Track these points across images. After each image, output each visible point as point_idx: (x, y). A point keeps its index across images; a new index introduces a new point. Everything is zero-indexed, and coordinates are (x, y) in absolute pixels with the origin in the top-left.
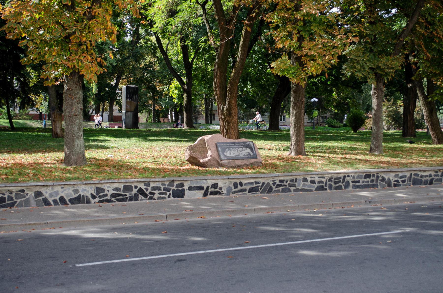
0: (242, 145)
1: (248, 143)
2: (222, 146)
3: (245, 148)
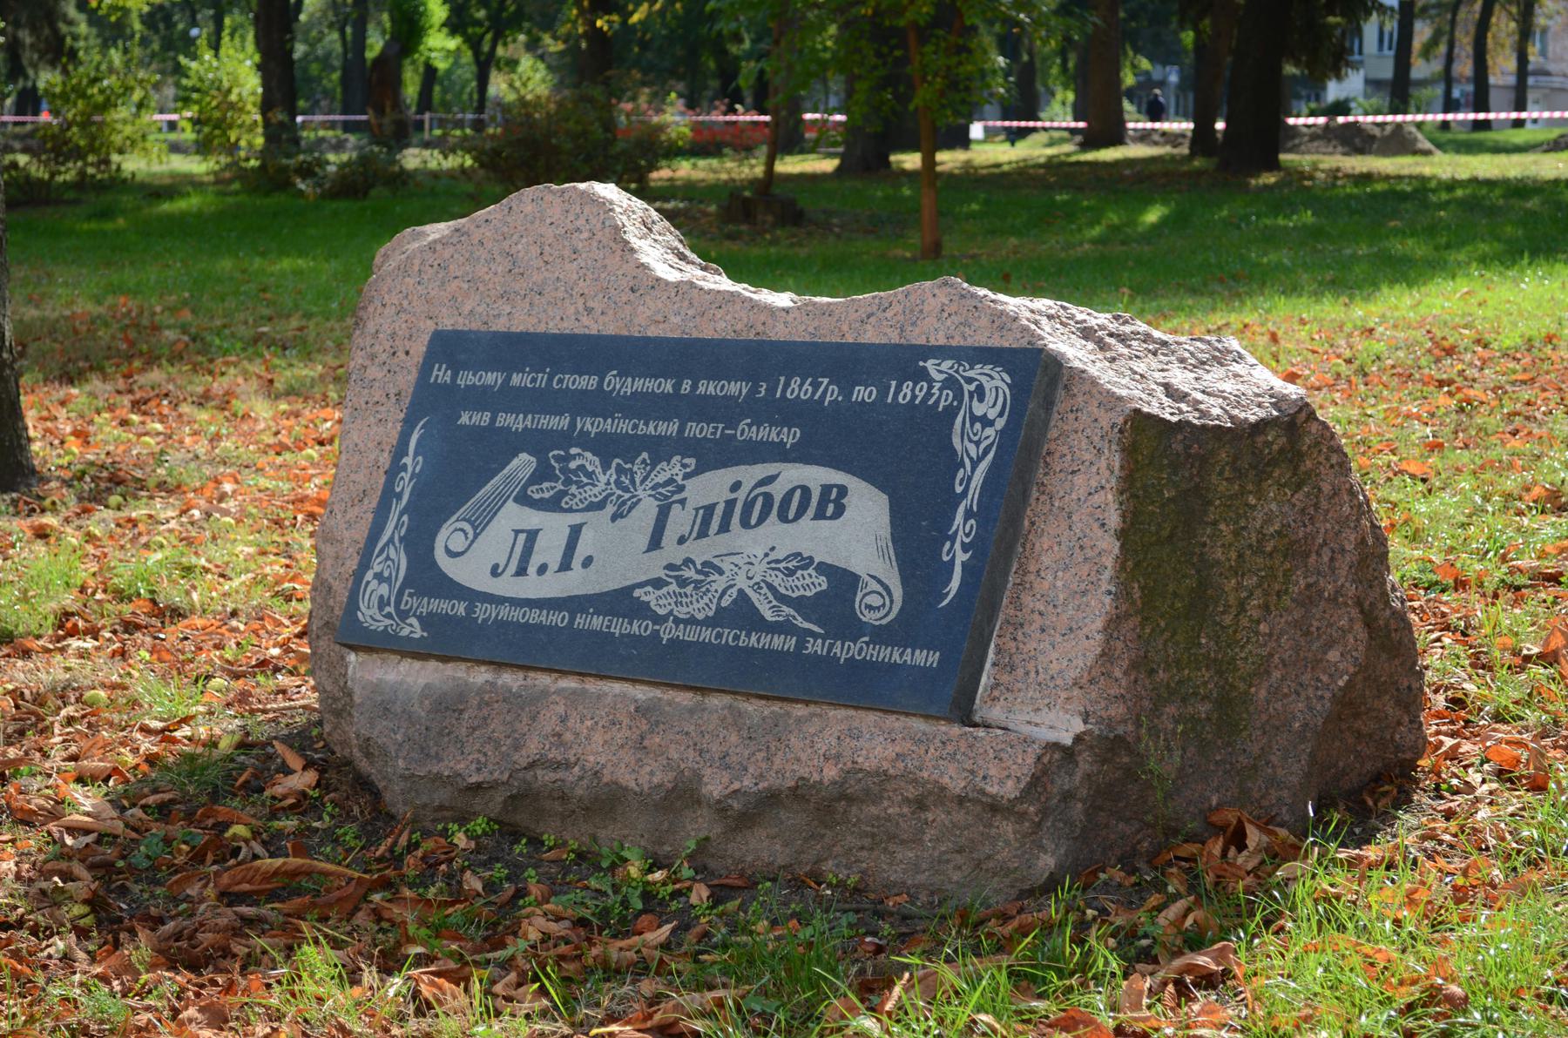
0: (787, 413)
1: (937, 369)
3: (816, 476)
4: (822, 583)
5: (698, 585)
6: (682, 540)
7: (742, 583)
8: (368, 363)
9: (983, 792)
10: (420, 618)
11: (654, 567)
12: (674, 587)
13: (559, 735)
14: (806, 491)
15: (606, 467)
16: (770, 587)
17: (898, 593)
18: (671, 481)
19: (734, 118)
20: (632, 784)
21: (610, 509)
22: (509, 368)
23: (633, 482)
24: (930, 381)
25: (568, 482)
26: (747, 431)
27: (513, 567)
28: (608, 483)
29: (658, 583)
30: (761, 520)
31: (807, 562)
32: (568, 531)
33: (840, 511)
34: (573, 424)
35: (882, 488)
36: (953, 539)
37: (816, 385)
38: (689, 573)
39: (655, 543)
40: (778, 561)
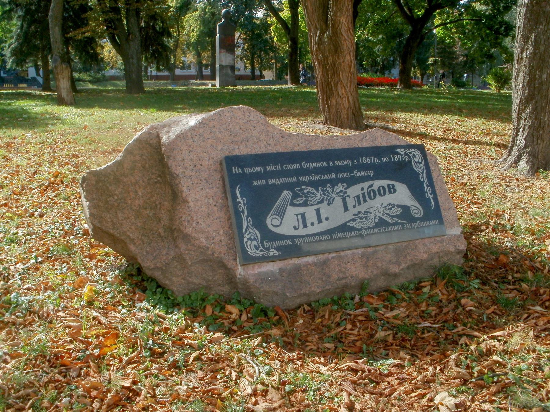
0: (366, 167)
1: (401, 151)
2: (258, 176)
3: (385, 183)
4: (400, 210)
5: (366, 218)
6: (354, 207)
7: (378, 215)
8: (185, 170)
9: (458, 250)
10: (275, 248)
11: (349, 216)
12: (359, 220)
13: (340, 270)
14: (383, 187)
15: (318, 191)
16: (387, 214)
17: (421, 208)
18: (341, 191)
19: (284, 86)
20: (367, 277)
21: (326, 203)
22: (264, 165)
23: (328, 193)
24: (401, 154)
25: (306, 197)
26: (357, 174)
27: (301, 225)
28: (321, 195)
29: (354, 220)
30: (375, 197)
31: (394, 206)
32: (315, 211)
33: (395, 191)
34: (298, 179)
35: (403, 183)
36: (427, 192)
37: (371, 159)
38: (361, 215)
39: (346, 209)
40: (385, 207)
